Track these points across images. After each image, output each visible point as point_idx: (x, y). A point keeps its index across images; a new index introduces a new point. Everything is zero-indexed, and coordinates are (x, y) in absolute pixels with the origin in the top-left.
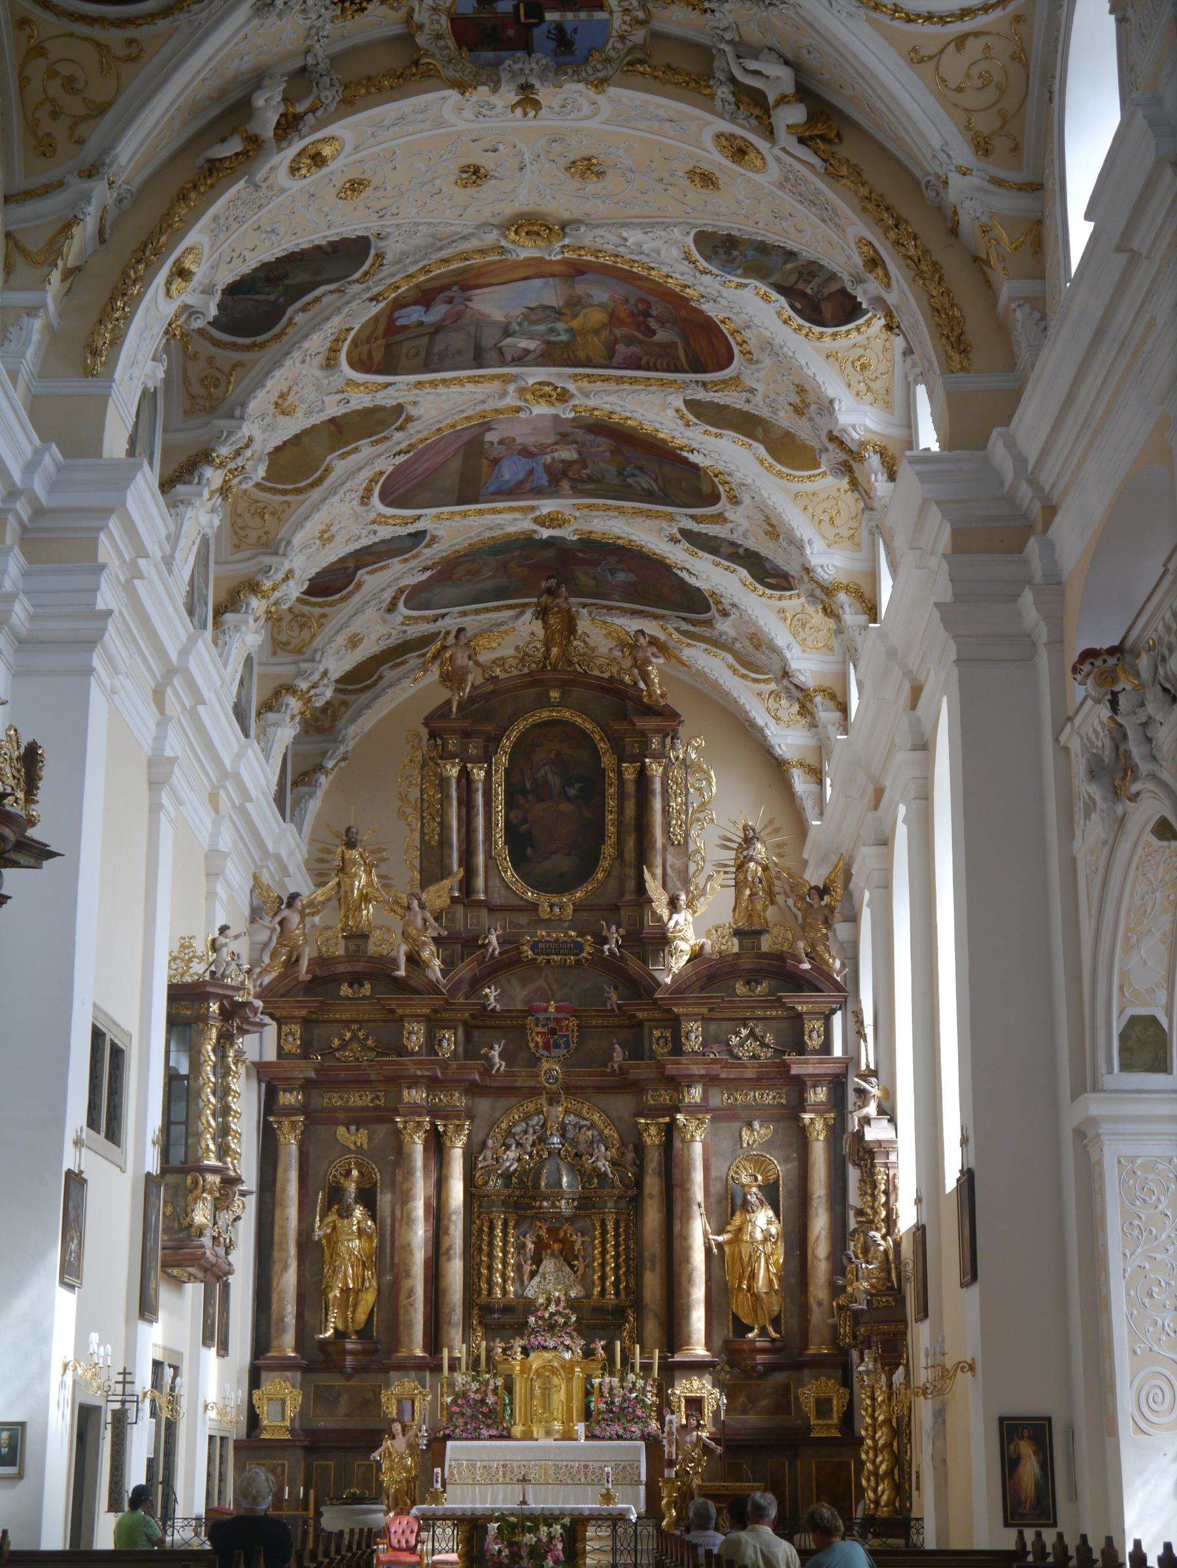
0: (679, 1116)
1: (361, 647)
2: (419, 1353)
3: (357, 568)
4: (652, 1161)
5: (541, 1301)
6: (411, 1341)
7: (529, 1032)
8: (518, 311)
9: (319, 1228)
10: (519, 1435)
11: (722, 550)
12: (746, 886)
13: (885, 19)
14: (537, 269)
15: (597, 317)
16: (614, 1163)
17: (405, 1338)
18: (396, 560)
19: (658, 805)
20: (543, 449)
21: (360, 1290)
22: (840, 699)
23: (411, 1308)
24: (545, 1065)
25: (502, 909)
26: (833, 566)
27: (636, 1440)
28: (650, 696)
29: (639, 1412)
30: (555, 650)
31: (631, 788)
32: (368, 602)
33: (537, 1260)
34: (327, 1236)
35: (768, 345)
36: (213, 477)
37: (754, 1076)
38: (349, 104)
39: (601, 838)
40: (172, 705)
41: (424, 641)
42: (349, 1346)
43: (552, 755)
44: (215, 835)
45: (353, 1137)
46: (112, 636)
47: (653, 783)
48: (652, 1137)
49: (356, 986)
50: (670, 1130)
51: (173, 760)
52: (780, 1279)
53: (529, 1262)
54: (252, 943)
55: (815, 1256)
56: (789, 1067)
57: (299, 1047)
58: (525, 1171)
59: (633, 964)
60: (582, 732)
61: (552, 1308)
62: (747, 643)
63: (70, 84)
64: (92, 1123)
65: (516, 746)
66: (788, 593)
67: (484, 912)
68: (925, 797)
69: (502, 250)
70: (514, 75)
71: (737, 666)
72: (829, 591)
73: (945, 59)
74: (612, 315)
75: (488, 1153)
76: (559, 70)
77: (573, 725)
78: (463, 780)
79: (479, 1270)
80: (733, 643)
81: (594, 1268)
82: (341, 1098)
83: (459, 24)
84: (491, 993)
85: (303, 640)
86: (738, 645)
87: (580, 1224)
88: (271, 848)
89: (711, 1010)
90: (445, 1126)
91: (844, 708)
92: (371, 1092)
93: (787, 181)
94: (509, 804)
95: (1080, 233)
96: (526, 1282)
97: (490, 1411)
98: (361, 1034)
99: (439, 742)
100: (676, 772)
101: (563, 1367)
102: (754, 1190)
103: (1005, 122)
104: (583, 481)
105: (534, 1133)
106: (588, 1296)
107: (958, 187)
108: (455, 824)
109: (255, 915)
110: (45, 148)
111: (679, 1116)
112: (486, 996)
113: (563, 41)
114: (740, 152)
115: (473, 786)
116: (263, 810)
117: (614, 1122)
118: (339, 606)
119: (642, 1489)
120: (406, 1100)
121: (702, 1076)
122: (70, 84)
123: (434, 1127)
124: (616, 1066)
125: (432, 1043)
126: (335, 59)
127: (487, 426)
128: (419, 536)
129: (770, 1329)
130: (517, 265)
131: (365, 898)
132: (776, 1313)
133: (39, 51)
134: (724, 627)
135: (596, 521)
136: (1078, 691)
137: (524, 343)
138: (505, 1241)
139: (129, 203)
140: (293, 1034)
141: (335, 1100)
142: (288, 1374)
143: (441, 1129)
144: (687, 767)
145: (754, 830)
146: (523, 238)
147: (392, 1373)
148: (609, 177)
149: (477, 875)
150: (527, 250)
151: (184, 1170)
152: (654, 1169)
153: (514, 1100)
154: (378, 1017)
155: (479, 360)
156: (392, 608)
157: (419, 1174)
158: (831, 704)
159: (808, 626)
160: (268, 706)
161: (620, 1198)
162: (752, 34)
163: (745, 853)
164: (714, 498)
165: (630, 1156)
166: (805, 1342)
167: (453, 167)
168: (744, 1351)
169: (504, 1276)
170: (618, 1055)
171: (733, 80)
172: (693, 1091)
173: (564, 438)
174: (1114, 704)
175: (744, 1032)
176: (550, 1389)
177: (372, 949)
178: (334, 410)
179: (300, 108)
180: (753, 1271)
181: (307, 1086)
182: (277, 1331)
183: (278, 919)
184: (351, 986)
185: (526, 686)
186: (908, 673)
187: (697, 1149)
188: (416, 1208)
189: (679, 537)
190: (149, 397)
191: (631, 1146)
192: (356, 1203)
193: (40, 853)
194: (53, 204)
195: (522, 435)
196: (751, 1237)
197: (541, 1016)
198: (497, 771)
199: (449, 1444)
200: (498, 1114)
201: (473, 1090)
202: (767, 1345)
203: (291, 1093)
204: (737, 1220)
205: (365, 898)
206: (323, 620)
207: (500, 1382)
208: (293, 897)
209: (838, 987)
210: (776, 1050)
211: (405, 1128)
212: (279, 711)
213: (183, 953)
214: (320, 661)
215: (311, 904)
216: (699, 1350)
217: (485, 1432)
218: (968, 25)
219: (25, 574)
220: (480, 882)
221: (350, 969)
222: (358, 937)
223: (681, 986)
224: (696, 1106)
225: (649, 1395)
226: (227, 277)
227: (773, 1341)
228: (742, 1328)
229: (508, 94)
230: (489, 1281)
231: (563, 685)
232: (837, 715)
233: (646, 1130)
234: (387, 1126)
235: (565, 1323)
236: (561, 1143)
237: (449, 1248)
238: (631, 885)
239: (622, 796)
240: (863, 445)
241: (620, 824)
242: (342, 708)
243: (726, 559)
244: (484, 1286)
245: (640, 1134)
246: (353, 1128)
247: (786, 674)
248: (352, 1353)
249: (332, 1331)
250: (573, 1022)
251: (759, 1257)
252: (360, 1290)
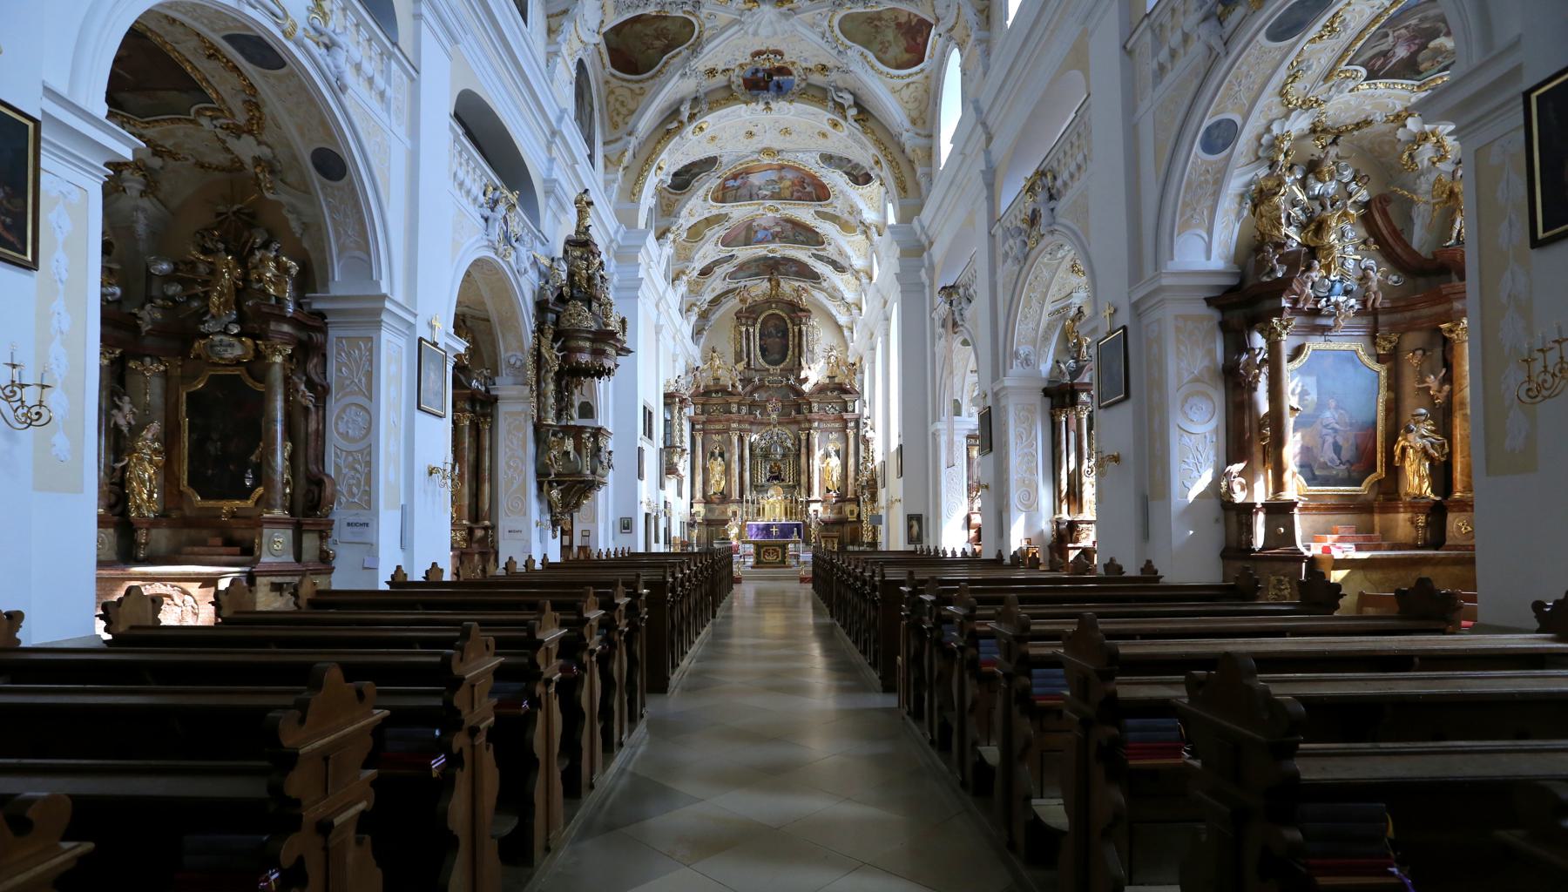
8: (763, 182)
13: (884, 78)
14: (770, 167)
15: (788, 183)
19: (805, 339)
20: (770, 228)
31: (797, 334)
35: (841, 192)
36: (671, 236)
38: (711, 110)
39: (788, 349)
40: (661, 309)
41: (734, 290)
44: (675, 349)
45: (717, 438)
46: (643, 286)
48: (803, 437)
50: (808, 434)
51: (662, 326)
63: (622, 103)
64: (644, 434)
68: (887, 335)
69: (759, 160)
70: (763, 99)
72: (857, 272)
73: (903, 92)
74: (793, 183)
76: (778, 97)
83: (746, 81)
84: (756, 395)
91: (860, 309)
93: (851, 135)
94: (760, 339)
95: (946, 148)
100: (810, 329)
103: (921, 114)
107: (905, 136)
109: (687, 373)
110: (615, 126)
113: (779, 87)
114: (835, 125)
116: (688, 341)
122: (622, 103)
125: (739, 411)
126: (706, 94)
127: (753, 220)
128: (732, 256)
130: (764, 165)
131: (719, 368)
133: (612, 92)
134: (825, 284)
136: (938, 299)
137: (767, 193)
139: (642, 145)
146: (766, 157)
148: (794, 136)
150: (766, 160)
151: (670, 447)
155: (751, 198)
156: (724, 279)
160: (688, 310)
162: (840, 84)
164: (823, 243)
167: (744, 132)
170: (793, 413)
171: (833, 100)
173: (777, 224)
174: (951, 304)
177: (721, 383)
178: (706, 215)
179: (695, 111)
181: (704, 423)
186: (883, 297)
187: (816, 441)
190: (650, 209)
193: (629, 351)
194: (619, 145)
195: (764, 223)
201: (752, 423)
205: (719, 368)
208: (698, 368)
213: (667, 384)
216: (816, 495)
218: (910, 80)
219: (616, 267)
220: (752, 362)
222: (717, 379)
223: (811, 394)
226: (673, 170)
229: (762, 106)
231: (776, 302)
239: (794, 336)
240: (871, 224)
241: (794, 345)
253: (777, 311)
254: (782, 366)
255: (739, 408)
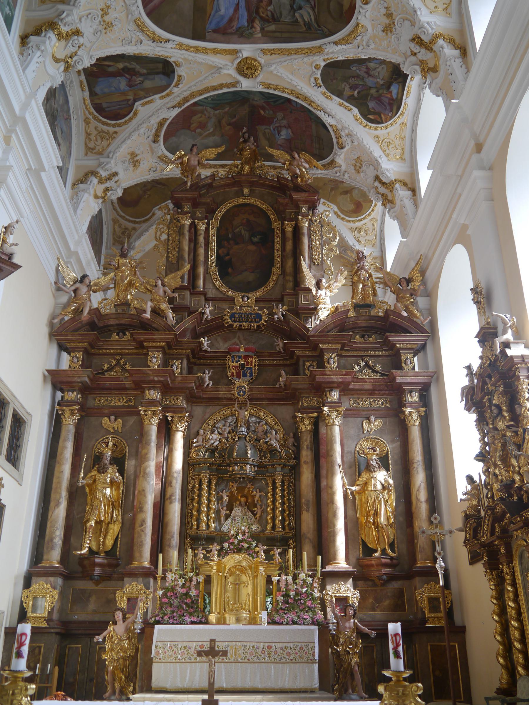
0: (325, 408)
1: (139, 170)
2: (146, 564)
3: (135, 101)
4: (306, 440)
5: (232, 532)
6: (141, 556)
7: (227, 366)
9: (83, 478)
10: (214, 621)
11: (345, 93)
12: (359, 281)
16: (281, 445)
17: (137, 554)
18: (158, 96)
19: (306, 241)
21: (109, 523)
22: (410, 186)
23: (142, 533)
24: (238, 383)
25: (214, 300)
26: (435, 23)
27: (308, 625)
28: (302, 180)
29: (309, 604)
30: (247, 167)
31: (289, 235)
32: (141, 124)
33: (230, 508)
34: (88, 485)
37: (371, 388)
39: (272, 263)
42: (97, 560)
43: (244, 221)
47: (303, 229)
48: (306, 426)
49: (121, 334)
52: (395, 517)
53: (225, 508)
54: (56, 304)
55: (419, 500)
56: (394, 379)
57: (81, 366)
58: (223, 449)
59: (293, 320)
60: (261, 210)
61: (240, 537)
62: (352, 170)
65: (223, 217)
66: (380, 126)
67: (202, 298)
71: (339, 213)
75: (200, 438)
77: (256, 206)
78: (193, 230)
79: (192, 513)
80: (344, 175)
81: (267, 512)
82: (107, 400)
84: (205, 342)
85: (103, 147)
86: (346, 176)
87: (257, 485)
88: (72, 248)
89: (342, 349)
90: (172, 417)
92: (126, 398)
94: (219, 246)
96: (223, 522)
97: (193, 602)
98: (122, 362)
99: (179, 210)
101: (250, 567)
102: (374, 457)
104: (268, 21)
105: (230, 426)
106: (264, 530)
108: (186, 248)
111: (325, 408)
112: (201, 343)
115: (198, 233)
117: (279, 421)
118: (124, 127)
119: (316, 666)
120: (146, 398)
121: (339, 384)
123: (165, 417)
124: (282, 384)
129: (389, 551)
132: (391, 540)
135: (274, 66)
138: (209, 494)
140: (78, 358)
141: (103, 402)
142: (52, 579)
143: (170, 419)
144: (322, 226)
145: (363, 253)
147: (126, 579)
149: (199, 279)
152: (307, 446)
153: (217, 408)
154: (134, 351)
157: (153, 445)
158: (405, 188)
159: (391, 146)
161: (284, 465)
163: (358, 265)
165: (291, 440)
166: (414, 560)
168: (372, 565)
169: (208, 516)
172: (333, 393)
175: (363, 364)
176: (239, 585)
180: (376, 510)
182: (47, 548)
183: (73, 288)
184: (118, 335)
185: (228, 185)
187: (337, 430)
188: (149, 466)
189: (321, 84)
191: (292, 434)
192: (111, 464)
196: (374, 487)
197: (235, 354)
198: (212, 229)
199: (157, 627)
200: (207, 416)
202: (388, 561)
203: (72, 393)
204: (365, 476)
206: (114, 135)
207: (201, 578)
208: (84, 277)
209: (423, 331)
210: (383, 375)
211: (145, 415)
212: (86, 184)
214: (112, 158)
215: (96, 285)
217: (187, 619)
220: (201, 283)
221: (117, 322)
224: (335, 403)
225: (316, 590)
227: (392, 558)
228: (369, 551)
230: (198, 520)
231: (252, 184)
232: (409, 193)
233: (302, 421)
234: (136, 417)
235: (248, 547)
236: (247, 432)
237: (172, 495)
238: (290, 285)
241: (283, 258)
242: (133, 231)
243: (346, 101)
244: (195, 523)
245: (297, 429)
246: (113, 418)
247: (377, 178)
248: (100, 565)
249: (87, 549)
250: (254, 360)
251: (380, 501)
252: (109, 523)
253: (253, 201)
254: (259, 293)
255: (165, 363)
